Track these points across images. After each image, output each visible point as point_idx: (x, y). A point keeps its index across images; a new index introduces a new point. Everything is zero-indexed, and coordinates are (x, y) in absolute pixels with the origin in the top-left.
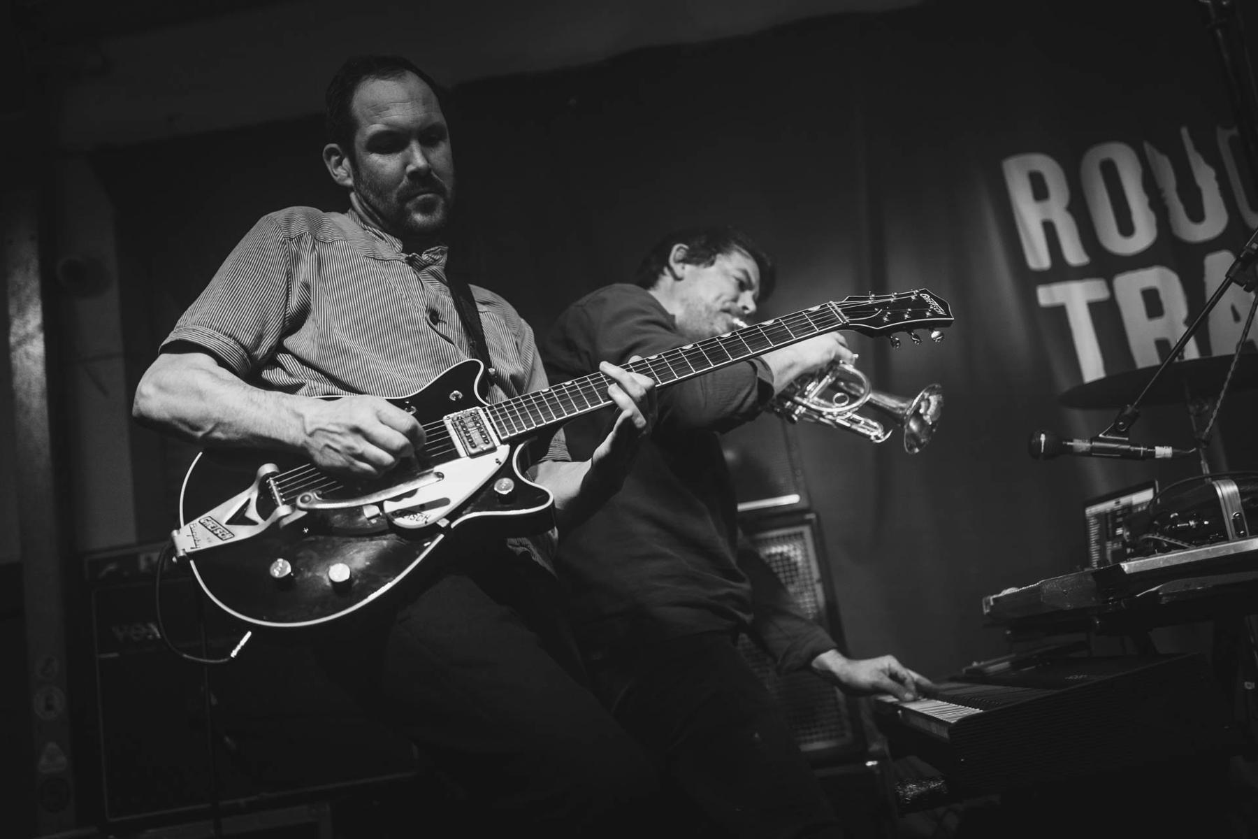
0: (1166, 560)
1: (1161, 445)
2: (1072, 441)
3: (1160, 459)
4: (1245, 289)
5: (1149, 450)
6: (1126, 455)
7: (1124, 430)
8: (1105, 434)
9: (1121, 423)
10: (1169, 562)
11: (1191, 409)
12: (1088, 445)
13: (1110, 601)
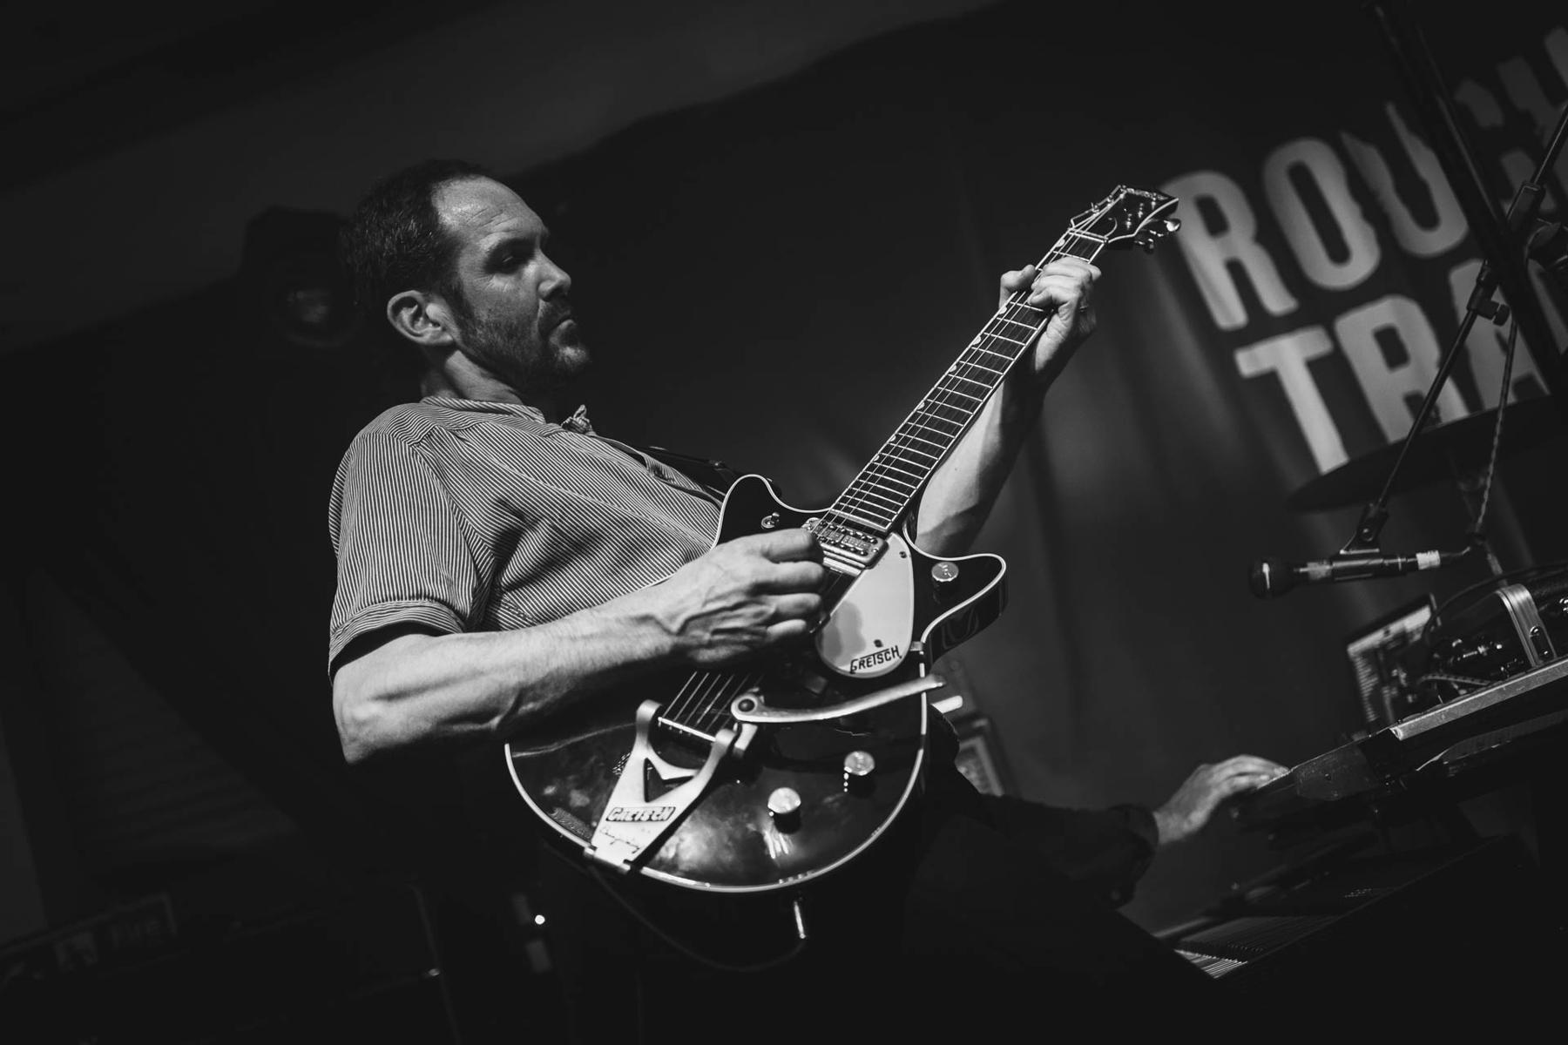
0: (1448, 714)
1: (1424, 551)
2: (1305, 566)
3: (1425, 570)
4: (1495, 323)
5: (1409, 560)
6: (1379, 572)
7: (1370, 539)
8: (1347, 549)
9: (1366, 531)
10: (1453, 714)
11: (1463, 486)
12: (1328, 567)
13: (1387, 780)
